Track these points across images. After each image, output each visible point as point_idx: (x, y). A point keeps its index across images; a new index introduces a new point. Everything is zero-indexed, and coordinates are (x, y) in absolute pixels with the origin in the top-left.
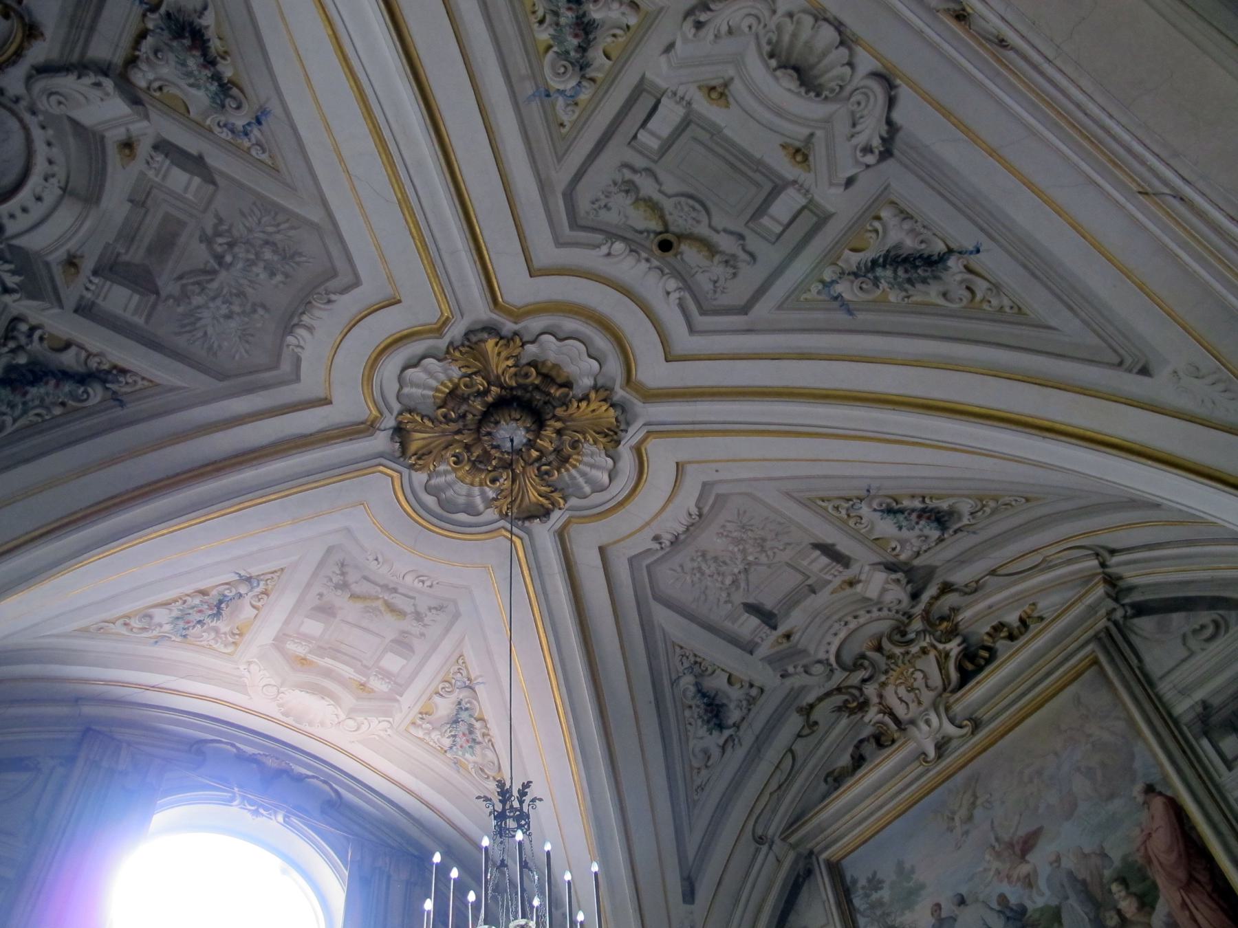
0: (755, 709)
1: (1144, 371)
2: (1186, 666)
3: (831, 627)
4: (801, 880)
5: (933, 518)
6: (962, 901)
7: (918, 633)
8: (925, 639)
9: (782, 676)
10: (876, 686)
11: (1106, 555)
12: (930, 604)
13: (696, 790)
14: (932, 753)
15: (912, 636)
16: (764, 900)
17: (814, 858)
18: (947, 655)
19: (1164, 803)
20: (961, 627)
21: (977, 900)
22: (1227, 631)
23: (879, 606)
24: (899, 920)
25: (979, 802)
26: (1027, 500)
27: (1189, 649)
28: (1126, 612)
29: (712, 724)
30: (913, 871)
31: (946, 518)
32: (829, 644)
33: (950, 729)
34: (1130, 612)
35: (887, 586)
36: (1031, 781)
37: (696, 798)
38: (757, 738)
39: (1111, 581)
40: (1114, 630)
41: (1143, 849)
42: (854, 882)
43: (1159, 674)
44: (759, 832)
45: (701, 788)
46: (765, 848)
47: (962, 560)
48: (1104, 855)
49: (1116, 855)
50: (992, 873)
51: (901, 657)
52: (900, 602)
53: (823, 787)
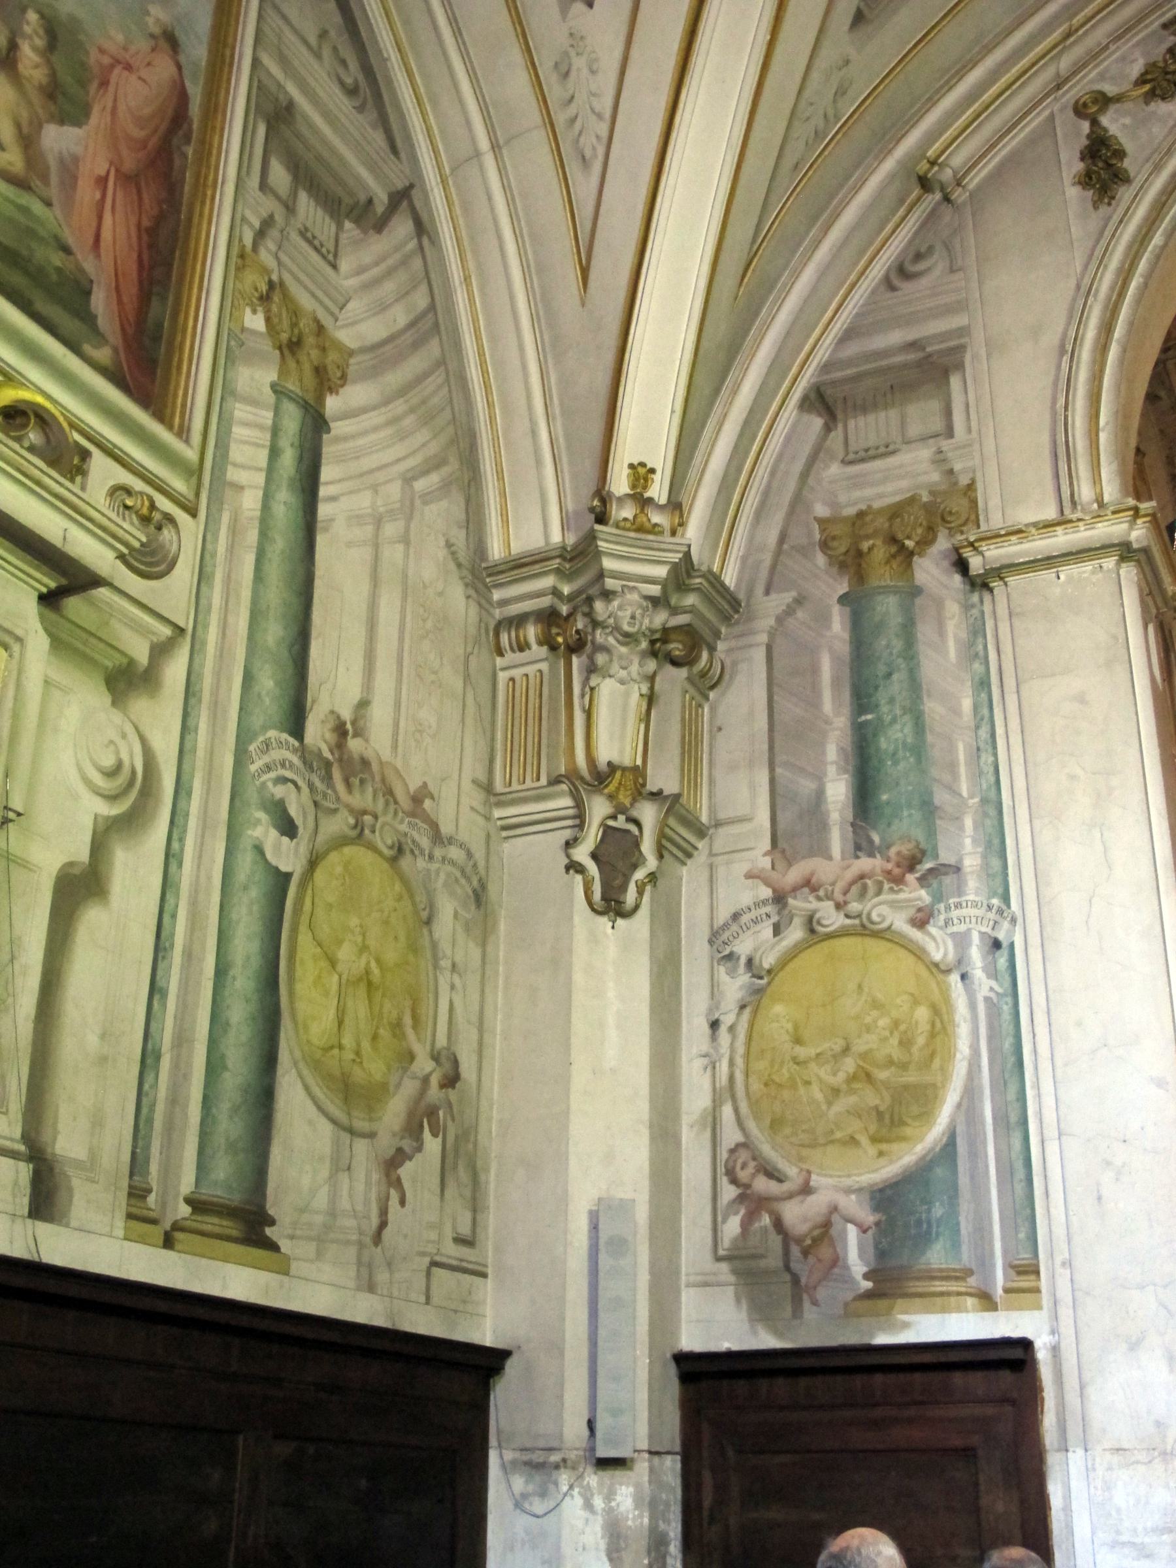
1: (859, 18)
2: (303, 49)
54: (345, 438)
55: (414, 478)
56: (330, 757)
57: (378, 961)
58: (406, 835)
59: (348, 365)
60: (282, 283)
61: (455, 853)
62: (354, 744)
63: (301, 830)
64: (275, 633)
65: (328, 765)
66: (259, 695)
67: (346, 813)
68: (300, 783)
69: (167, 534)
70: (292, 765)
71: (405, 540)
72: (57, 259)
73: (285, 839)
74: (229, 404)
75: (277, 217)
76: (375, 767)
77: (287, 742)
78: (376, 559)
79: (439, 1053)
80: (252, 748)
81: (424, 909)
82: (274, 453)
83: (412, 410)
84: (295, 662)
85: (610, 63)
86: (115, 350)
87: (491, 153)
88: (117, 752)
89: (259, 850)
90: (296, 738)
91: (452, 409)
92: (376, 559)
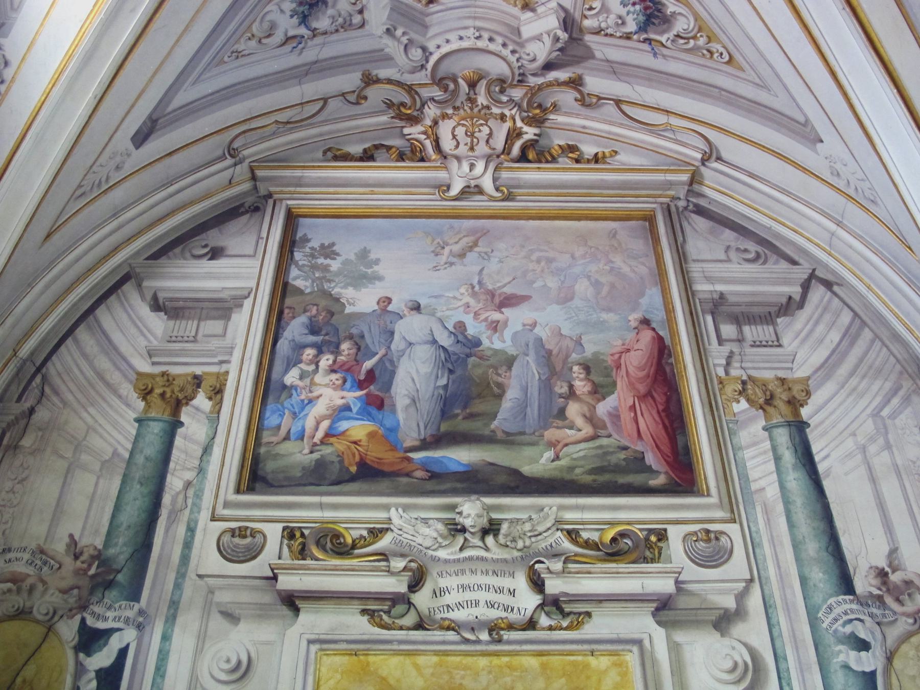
0: (342, 35)
2: (720, 265)
3: (466, 28)
4: (242, 210)
5: (648, 12)
6: (417, 308)
7: (511, 100)
8: (511, 110)
9: (388, 30)
10: (438, 112)
11: (714, 156)
12: (550, 85)
13: (233, 52)
14: (455, 191)
15: (504, 99)
16: (192, 203)
17: (271, 202)
18: (520, 134)
19: (654, 338)
20: (547, 124)
21: (433, 314)
22: (765, 263)
23: (517, 48)
24: (337, 290)
25: (477, 249)
26: (731, 61)
27: (728, 257)
28: (688, 206)
29: (301, 9)
30: (377, 262)
31: (656, 22)
32: (448, 41)
33: (487, 184)
34: (691, 207)
35: (545, 37)
36: (538, 261)
37: (226, 59)
38: (316, 62)
39: (695, 179)
40: (673, 209)
41: (617, 356)
42: (306, 240)
43: (695, 258)
44: (236, 145)
45: (238, 55)
46: (229, 161)
47: (614, 69)
48: (579, 342)
49: (590, 349)
50: (460, 303)
51: (480, 107)
52: (534, 60)
53: (320, 154)
54: (816, 426)
55: (881, 410)
56: (878, 592)
59: (808, 386)
60: (750, 377)
62: (895, 578)
63: (873, 643)
64: (813, 547)
65: (880, 598)
66: (815, 585)
67: (904, 618)
68: (862, 617)
69: (723, 539)
70: (852, 611)
71: (888, 446)
72: (622, 455)
73: (863, 653)
74: (740, 454)
75: (734, 350)
77: (844, 600)
78: (870, 469)
80: (820, 615)
82: (777, 459)
83: (864, 377)
84: (833, 556)
85: (847, 157)
86: (666, 473)
87: (839, 229)
88: (732, 658)
89: (846, 667)
90: (850, 594)
91: (895, 356)
92: (870, 469)
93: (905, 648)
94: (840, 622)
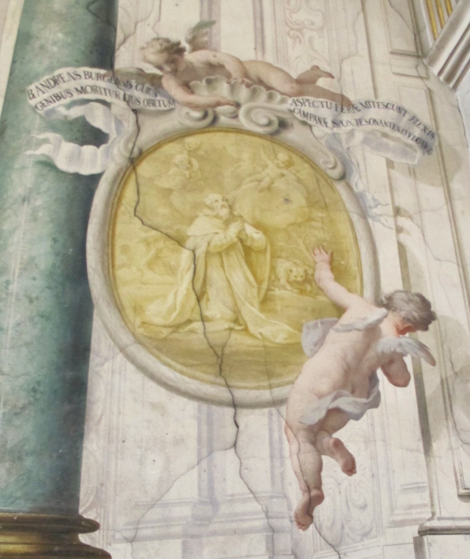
56: (158, 72)
57: (258, 226)
58: (292, 112)
61: (373, 113)
62: (190, 57)
63: (113, 135)
66: (42, 47)
67: (186, 110)
68: (108, 99)
70: (94, 89)
73: (88, 149)
76: (231, 67)
79: (390, 298)
80: (32, 87)
81: (334, 168)
93: (169, 148)
94: (63, 101)
